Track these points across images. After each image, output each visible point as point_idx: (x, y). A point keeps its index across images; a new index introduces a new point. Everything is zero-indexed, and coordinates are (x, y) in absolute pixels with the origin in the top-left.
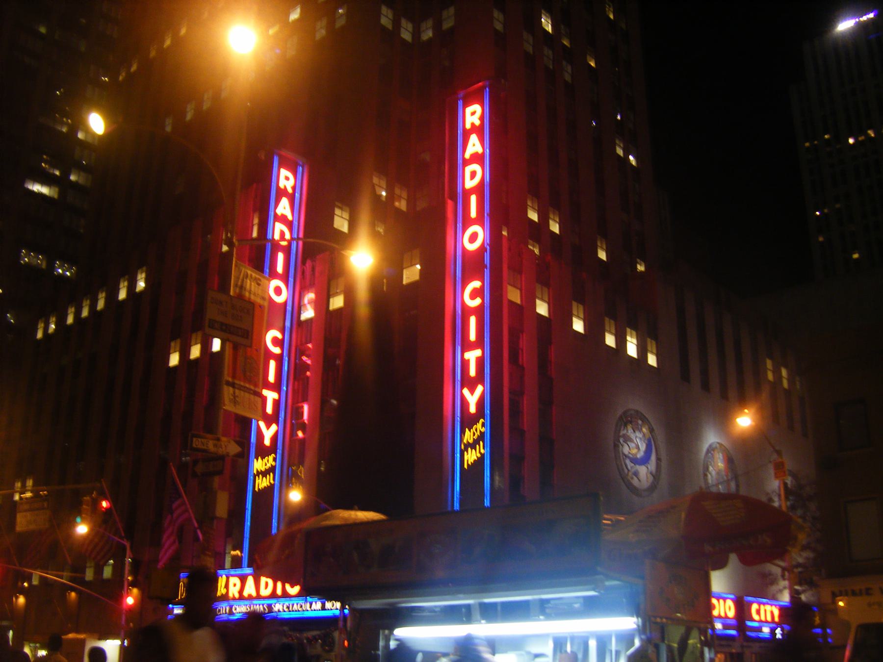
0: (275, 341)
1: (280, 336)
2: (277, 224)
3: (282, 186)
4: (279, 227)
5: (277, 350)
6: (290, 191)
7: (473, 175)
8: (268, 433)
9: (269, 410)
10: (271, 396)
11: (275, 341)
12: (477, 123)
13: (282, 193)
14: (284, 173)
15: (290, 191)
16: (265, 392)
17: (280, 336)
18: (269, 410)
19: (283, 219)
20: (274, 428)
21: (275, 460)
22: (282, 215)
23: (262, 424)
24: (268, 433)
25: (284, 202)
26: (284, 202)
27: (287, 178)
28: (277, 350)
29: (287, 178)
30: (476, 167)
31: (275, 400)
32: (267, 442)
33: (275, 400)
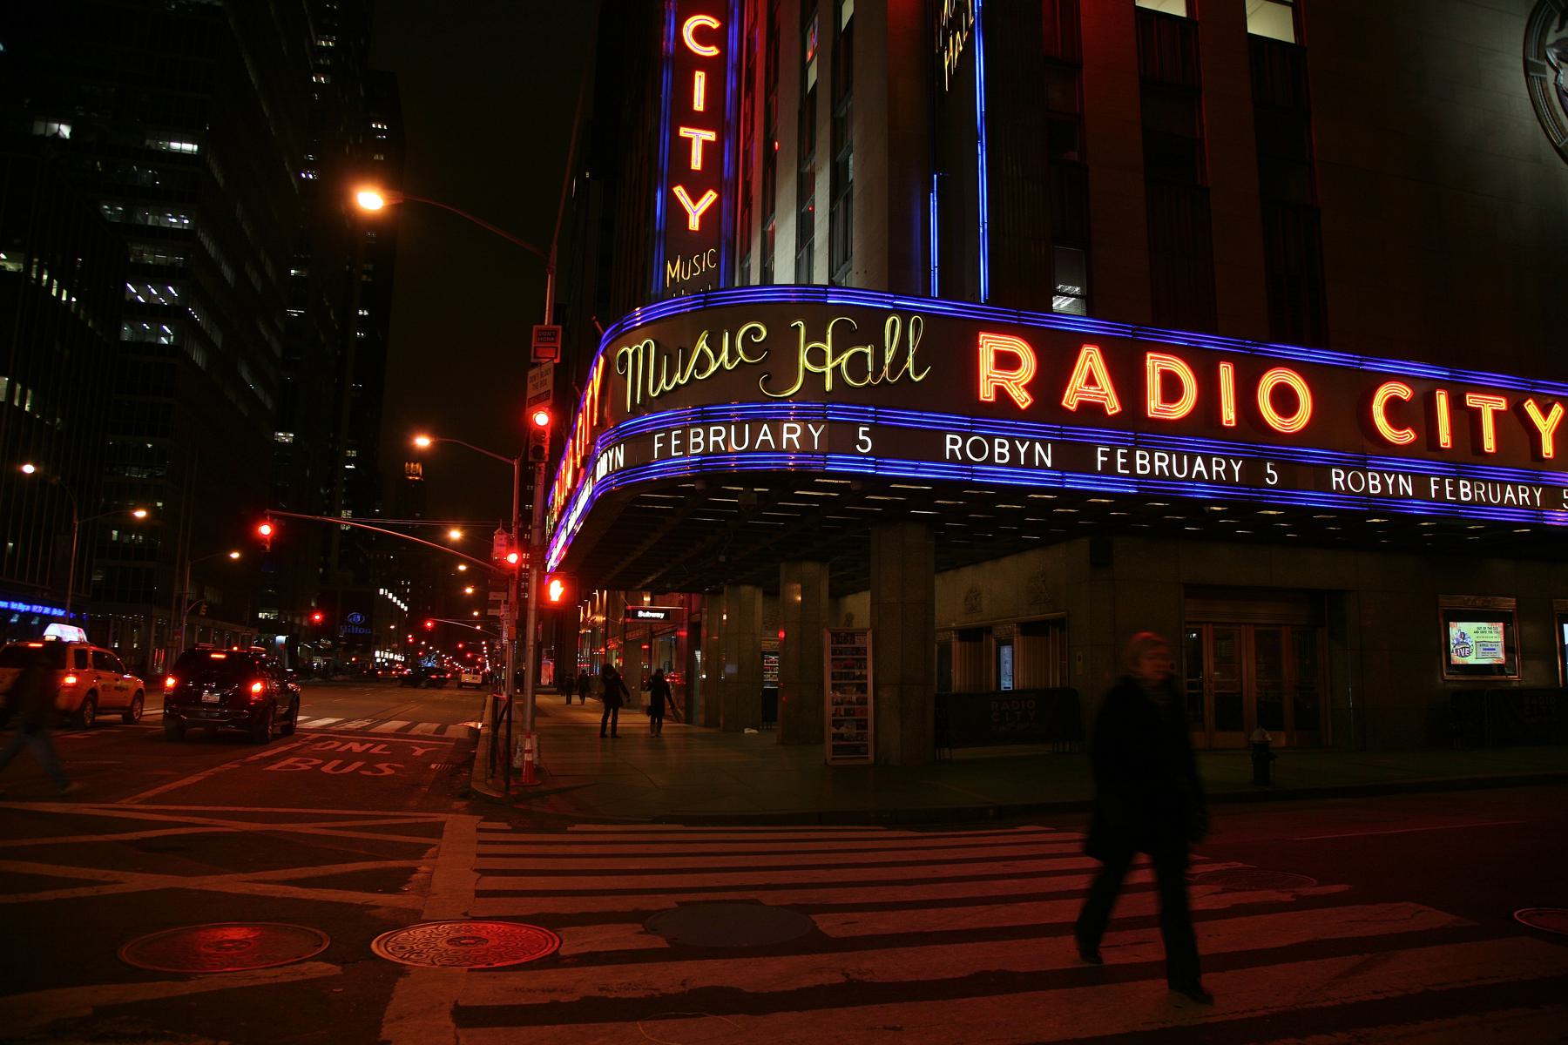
0: (702, 34)
1: (715, 24)
5: (712, 51)
8: (695, 212)
9: (696, 163)
10: (699, 138)
11: (702, 34)
16: (684, 132)
17: (715, 24)
18: (696, 163)
20: (710, 197)
21: (715, 258)
23: (679, 191)
24: (695, 212)
28: (712, 51)
31: (705, 143)
32: (694, 224)
33: (705, 143)
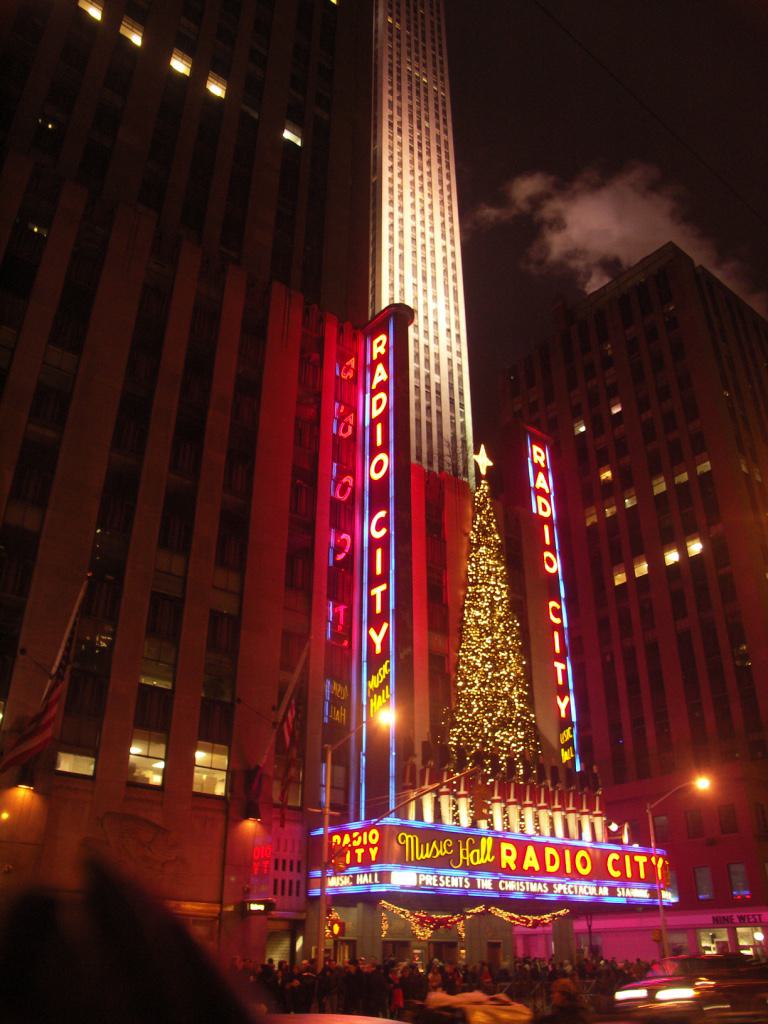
2: (539, 498)
3: (536, 461)
4: (541, 500)
6: (543, 465)
7: (379, 402)
12: (382, 350)
13: (537, 468)
14: (536, 449)
15: (543, 465)
19: (540, 492)
22: (541, 488)
25: (541, 476)
26: (541, 476)
27: (539, 454)
29: (539, 454)
30: (382, 396)
